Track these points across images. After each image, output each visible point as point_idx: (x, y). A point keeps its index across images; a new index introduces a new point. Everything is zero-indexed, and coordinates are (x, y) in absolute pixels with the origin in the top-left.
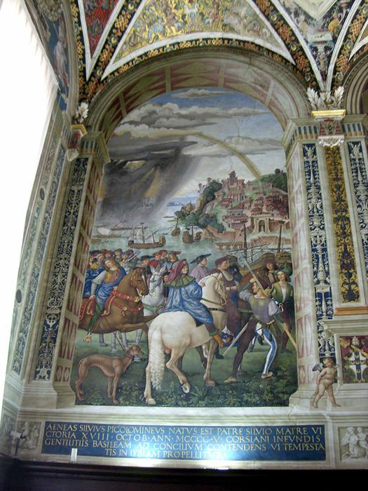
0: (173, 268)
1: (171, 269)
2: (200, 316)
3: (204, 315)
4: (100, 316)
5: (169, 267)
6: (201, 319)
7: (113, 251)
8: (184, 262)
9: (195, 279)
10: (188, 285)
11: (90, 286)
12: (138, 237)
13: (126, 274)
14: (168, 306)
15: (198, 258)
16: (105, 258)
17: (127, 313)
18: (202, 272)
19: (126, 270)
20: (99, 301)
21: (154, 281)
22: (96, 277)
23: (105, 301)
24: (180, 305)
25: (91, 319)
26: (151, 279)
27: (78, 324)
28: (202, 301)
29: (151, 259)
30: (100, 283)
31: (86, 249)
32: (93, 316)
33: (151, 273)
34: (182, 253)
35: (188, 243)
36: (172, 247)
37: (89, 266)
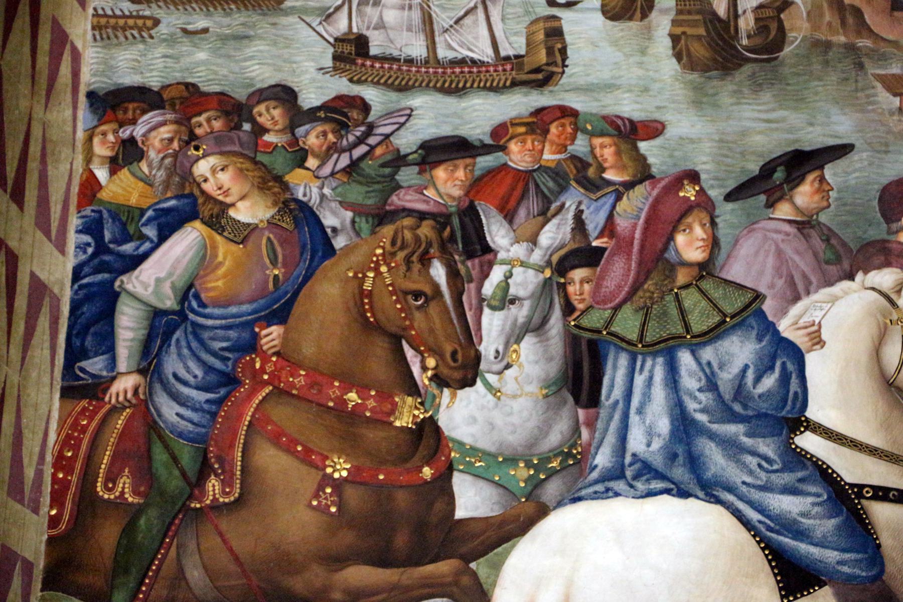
0: (622, 224)
1: (609, 228)
2: (800, 534)
3: (826, 526)
4: (185, 509)
5: (595, 221)
6: (803, 548)
7: (241, 95)
8: (689, 192)
9: (758, 297)
10: (714, 334)
11: (108, 314)
12: (391, 16)
13: (329, 251)
14: (603, 459)
15: (767, 170)
16: (193, 137)
17: (352, 495)
18: (802, 263)
19: (329, 220)
20: (169, 410)
21: (505, 300)
22: (136, 261)
23: (214, 415)
24: (672, 457)
25: (130, 529)
26: (488, 288)
27: (41, 564)
28: (808, 442)
29: (485, 162)
30: (169, 303)
31: (65, 69)
32: (138, 511)
33: (487, 249)
34: (671, 132)
35: (705, 69)
36: (609, 87)
37: (90, 186)
